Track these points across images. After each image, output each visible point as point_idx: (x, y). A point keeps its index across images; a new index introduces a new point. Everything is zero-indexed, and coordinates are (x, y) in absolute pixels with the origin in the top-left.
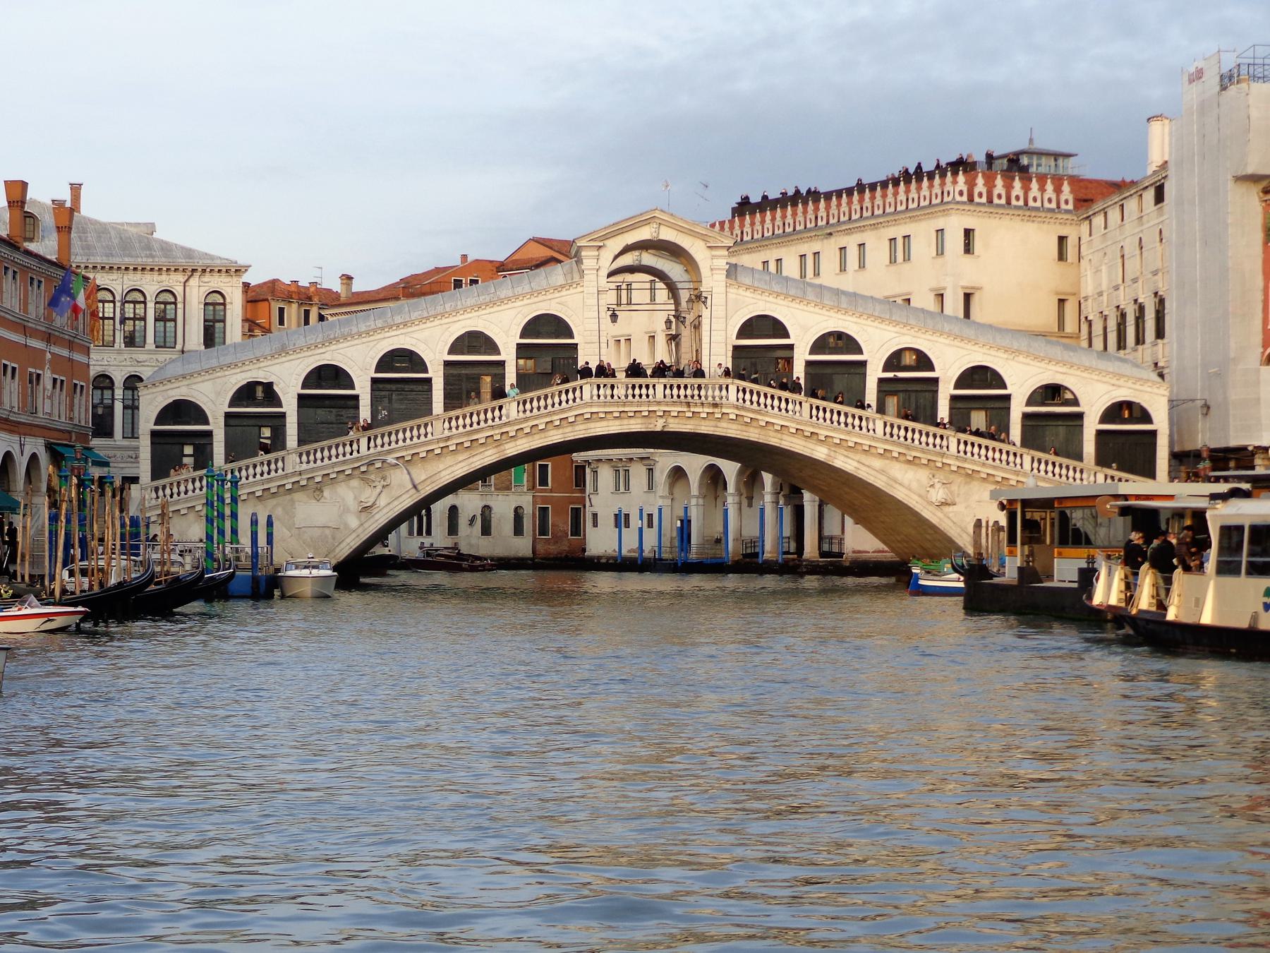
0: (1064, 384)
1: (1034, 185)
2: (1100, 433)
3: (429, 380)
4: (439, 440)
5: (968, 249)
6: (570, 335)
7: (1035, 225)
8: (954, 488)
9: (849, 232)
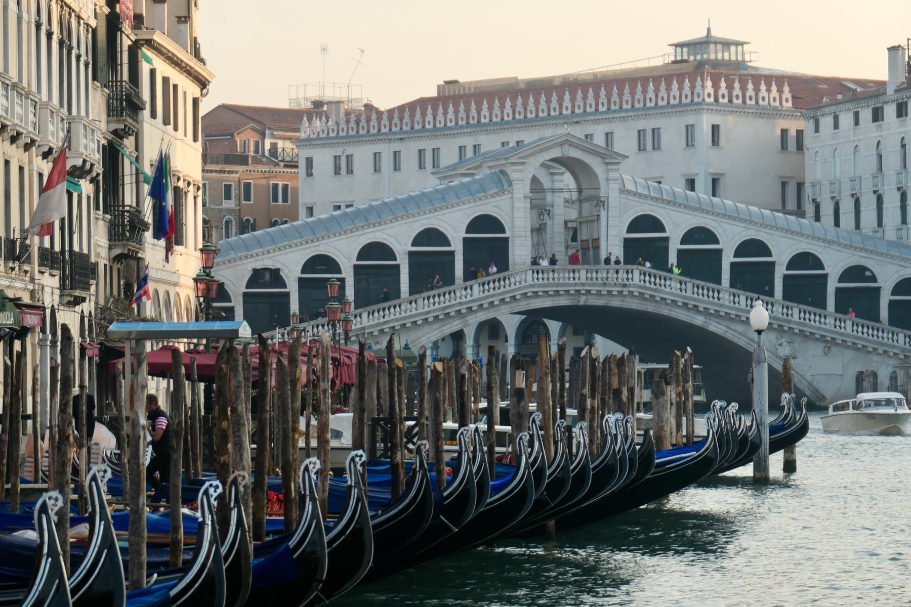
0: (866, 265)
1: (763, 87)
2: (891, 303)
3: (397, 267)
4: (421, 314)
5: (715, 141)
6: (503, 231)
7: (764, 120)
8: (796, 345)
9: (597, 122)
